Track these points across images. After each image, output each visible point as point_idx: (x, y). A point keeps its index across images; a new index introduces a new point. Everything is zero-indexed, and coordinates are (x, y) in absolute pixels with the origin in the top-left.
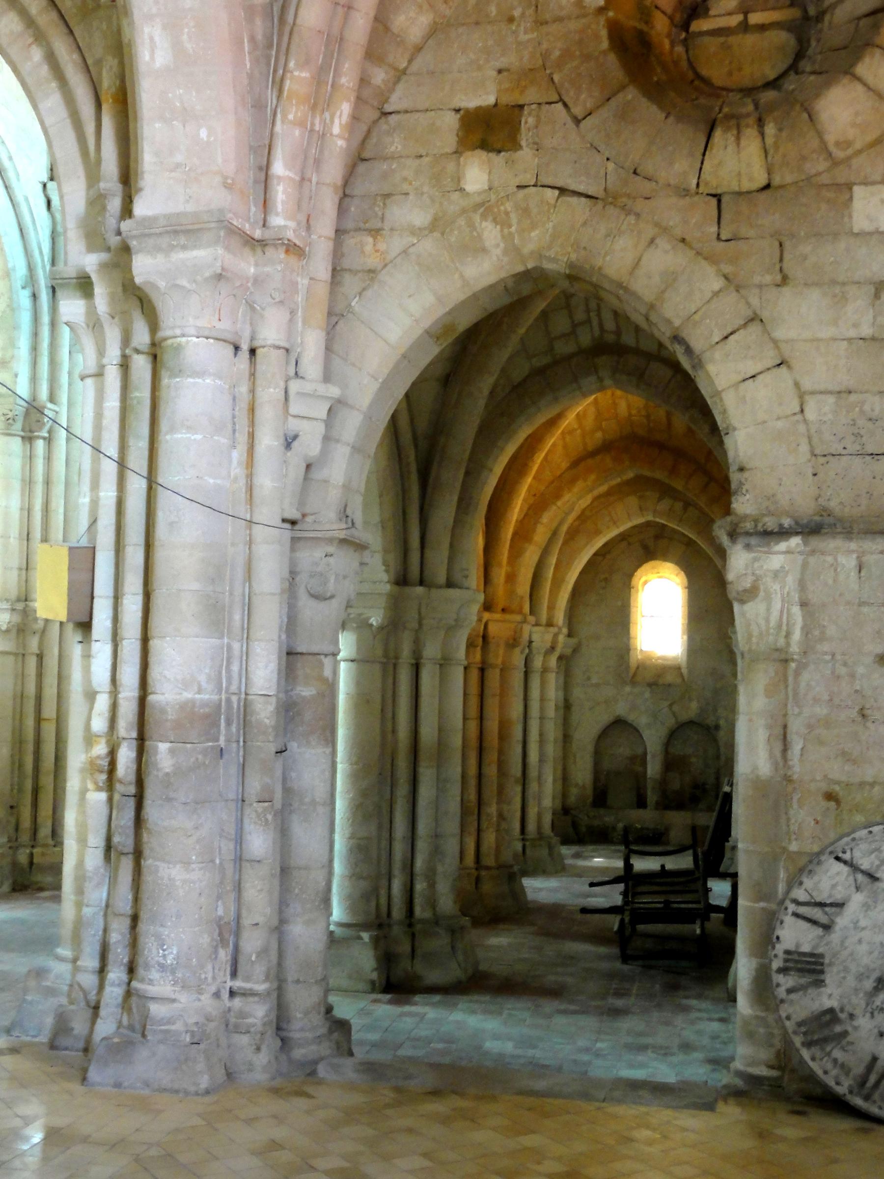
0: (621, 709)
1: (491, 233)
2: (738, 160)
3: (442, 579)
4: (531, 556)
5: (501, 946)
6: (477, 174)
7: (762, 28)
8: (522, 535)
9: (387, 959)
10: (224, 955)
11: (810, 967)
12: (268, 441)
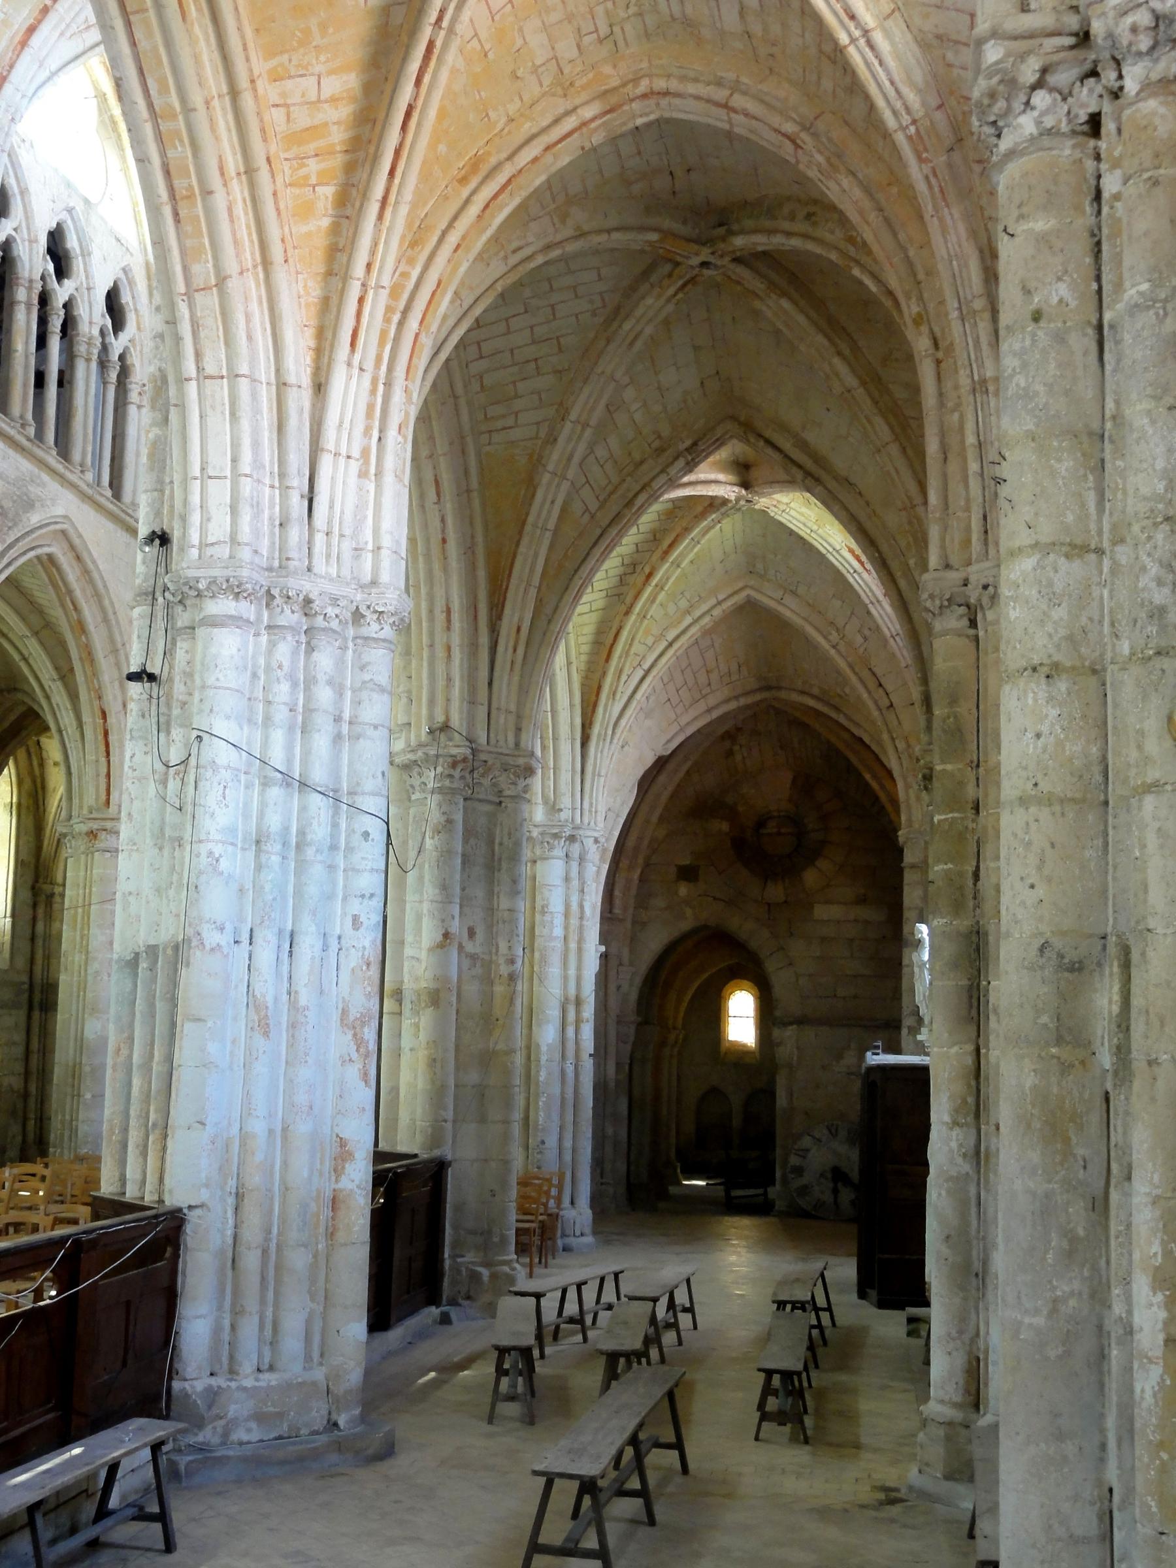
1: (689, 912)
2: (776, 892)
6: (683, 890)
11: (799, 1171)
12: (612, 987)
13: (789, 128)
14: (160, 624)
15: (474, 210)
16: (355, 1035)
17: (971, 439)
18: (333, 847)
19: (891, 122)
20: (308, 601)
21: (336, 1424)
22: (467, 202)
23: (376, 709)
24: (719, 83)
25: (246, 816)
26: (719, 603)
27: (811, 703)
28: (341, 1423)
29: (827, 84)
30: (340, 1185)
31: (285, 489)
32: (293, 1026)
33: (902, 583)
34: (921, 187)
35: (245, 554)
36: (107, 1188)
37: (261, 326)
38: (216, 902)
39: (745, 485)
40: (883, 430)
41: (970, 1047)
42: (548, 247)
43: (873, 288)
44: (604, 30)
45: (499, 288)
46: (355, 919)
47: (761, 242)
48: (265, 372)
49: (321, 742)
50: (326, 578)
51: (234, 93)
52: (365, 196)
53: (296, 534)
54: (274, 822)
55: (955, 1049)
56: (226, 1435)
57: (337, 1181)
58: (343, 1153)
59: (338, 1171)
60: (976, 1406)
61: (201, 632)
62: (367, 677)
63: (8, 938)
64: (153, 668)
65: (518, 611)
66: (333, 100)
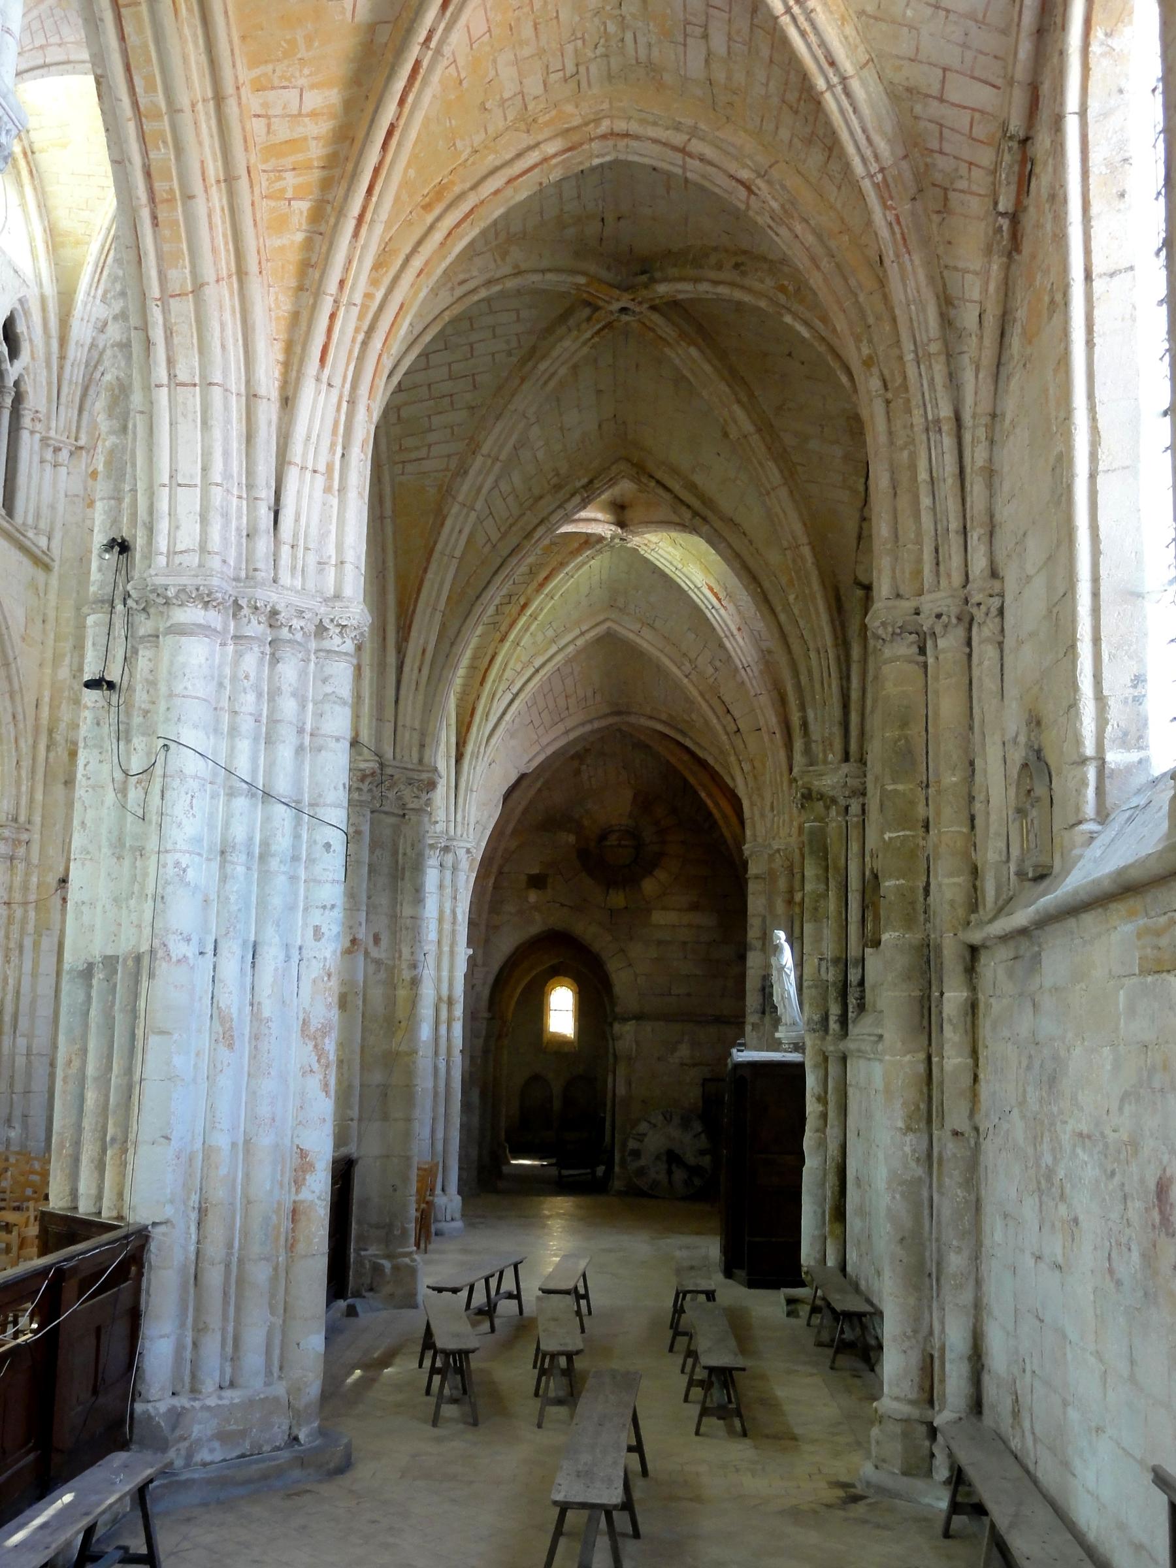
1: (537, 916)
2: (618, 899)
6: (533, 896)
11: (636, 1154)
13: (745, 174)
14: (119, 630)
15: (438, 236)
16: (316, 1046)
17: (923, 476)
18: (295, 858)
19: (859, 169)
20: (274, 613)
21: (296, 1439)
22: (431, 228)
23: (339, 722)
24: (677, 127)
25: (211, 827)
26: (582, 634)
27: (660, 727)
28: (302, 1437)
29: (784, 134)
30: (301, 1197)
31: (253, 500)
32: (256, 1037)
33: (783, 617)
34: (884, 233)
35: (215, 563)
36: (57, 1202)
37: (231, 337)
38: (183, 913)
39: (621, 524)
40: (773, 473)
41: (922, 1056)
42: (489, 283)
43: (805, 333)
44: (570, 68)
45: (447, 317)
46: (317, 929)
47: (684, 290)
48: (236, 382)
49: (285, 752)
50: (290, 592)
51: (219, 99)
52: (341, 213)
53: (263, 544)
54: (239, 832)
55: (908, 1057)
56: (189, 1456)
57: (297, 1192)
58: (304, 1164)
59: (298, 1183)
60: (931, 1402)
61: (167, 642)
62: (328, 689)
64: (113, 675)
65: (424, 633)
66: (313, 114)
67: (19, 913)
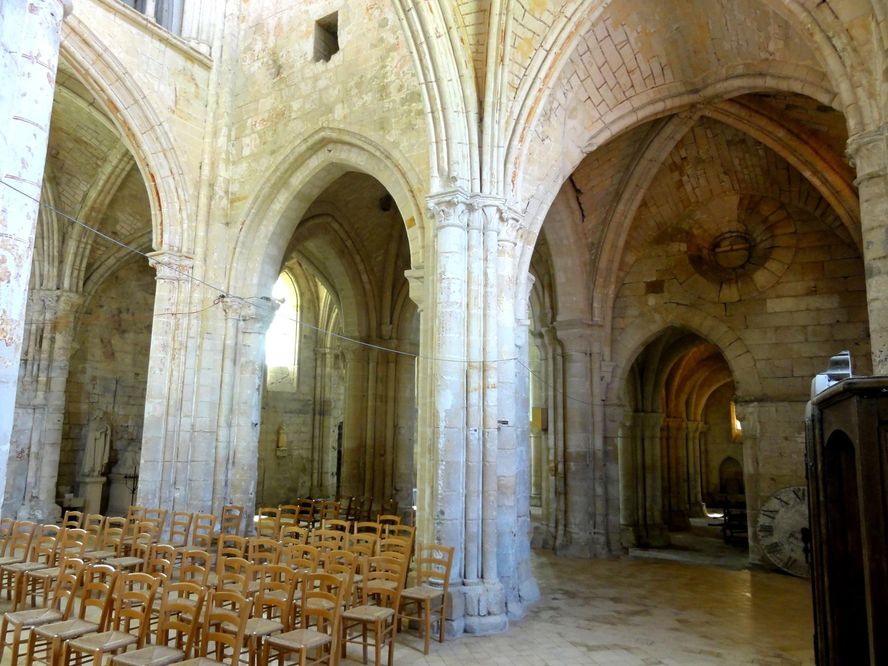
0: (730, 453)
1: (657, 317)
2: (730, 293)
3: (649, 410)
4: (684, 398)
5: (679, 538)
6: (652, 300)
7: (737, 250)
8: (680, 389)
9: (638, 538)
10: (592, 522)
11: (768, 530)
12: (596, 379)
63: (296, 375)
67: (184, 322)
